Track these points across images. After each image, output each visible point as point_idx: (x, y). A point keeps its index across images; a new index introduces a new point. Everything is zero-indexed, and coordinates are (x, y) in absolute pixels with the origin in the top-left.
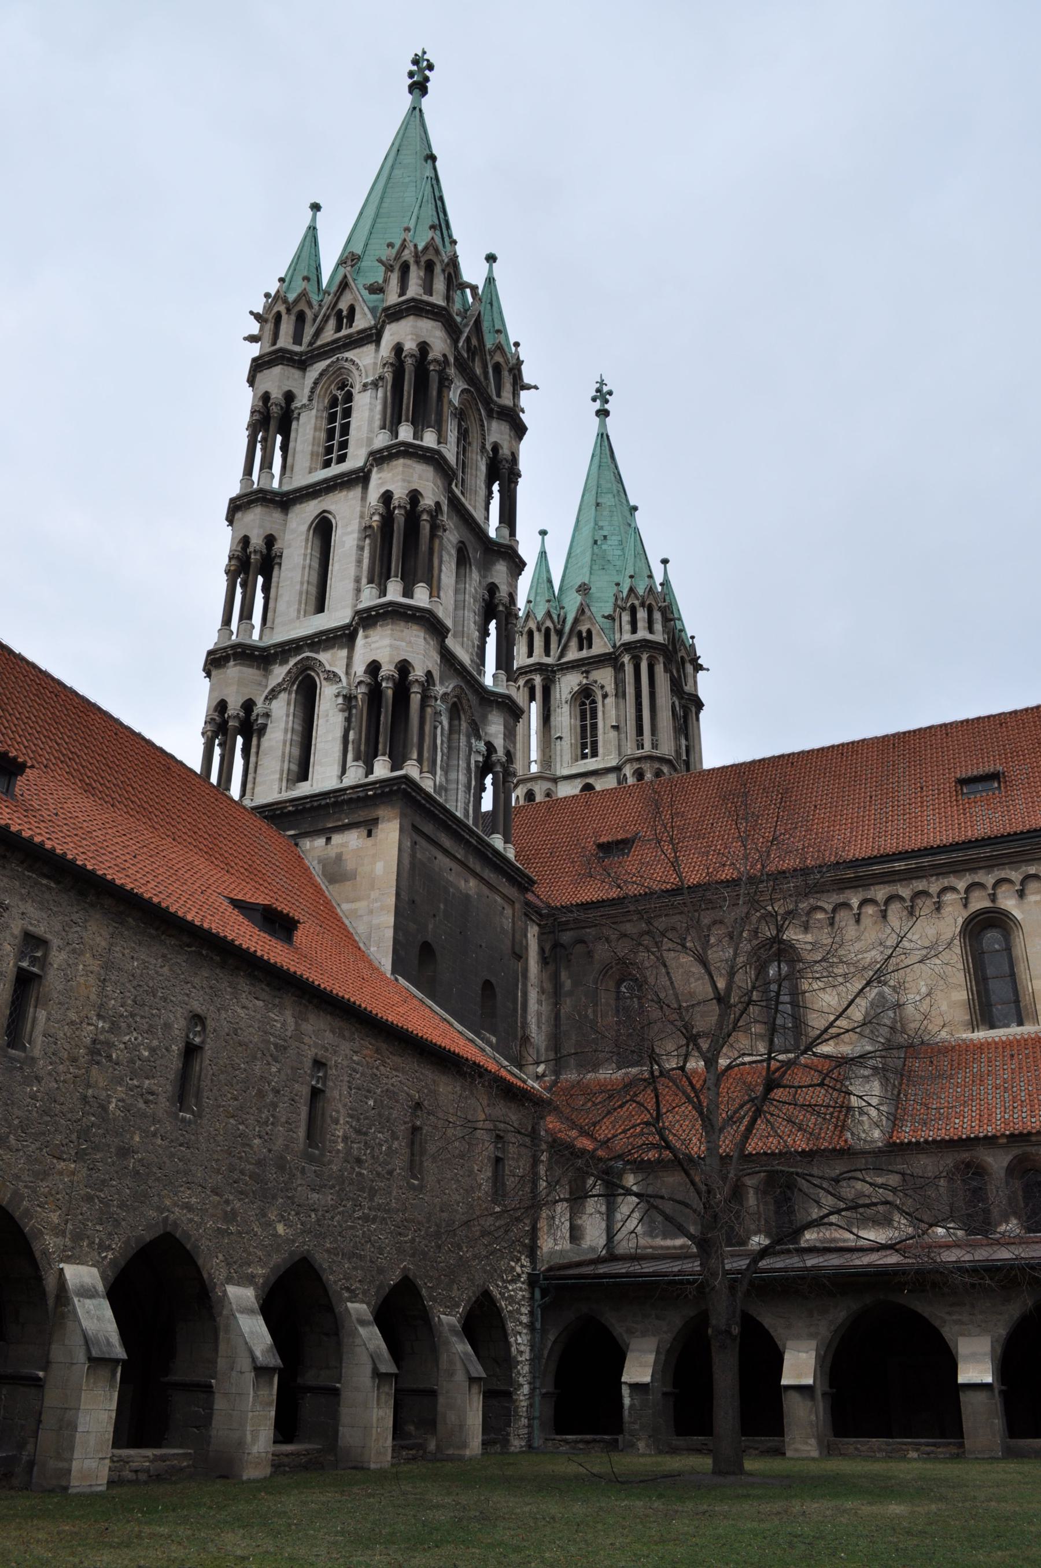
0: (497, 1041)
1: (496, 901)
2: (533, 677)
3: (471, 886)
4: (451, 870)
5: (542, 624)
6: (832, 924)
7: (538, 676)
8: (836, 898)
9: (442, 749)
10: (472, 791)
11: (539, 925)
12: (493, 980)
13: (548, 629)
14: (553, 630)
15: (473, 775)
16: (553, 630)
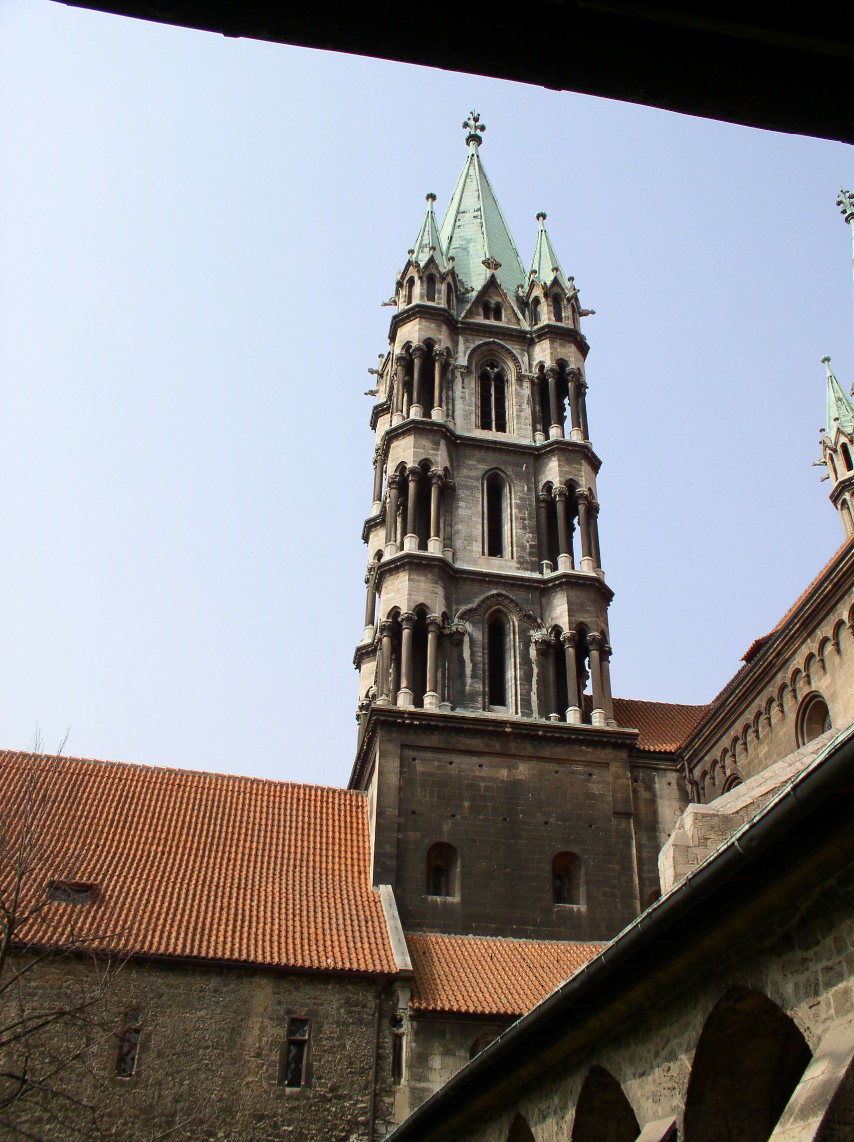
0: (589, 910)
1: (573, 772)
2: (844, 497)
3: (523, 770)
4: (481, 766)
5: (836, 444)
6: (838, 651)
7: (846, 493)
8: (833, 619)
9: (472, 661)
10: (535, 679)
11: (676, 771)
12: (576, 850)
13: (844, 446)
14: (848, 443)
15: (534, 666)
16: (848, 443)
